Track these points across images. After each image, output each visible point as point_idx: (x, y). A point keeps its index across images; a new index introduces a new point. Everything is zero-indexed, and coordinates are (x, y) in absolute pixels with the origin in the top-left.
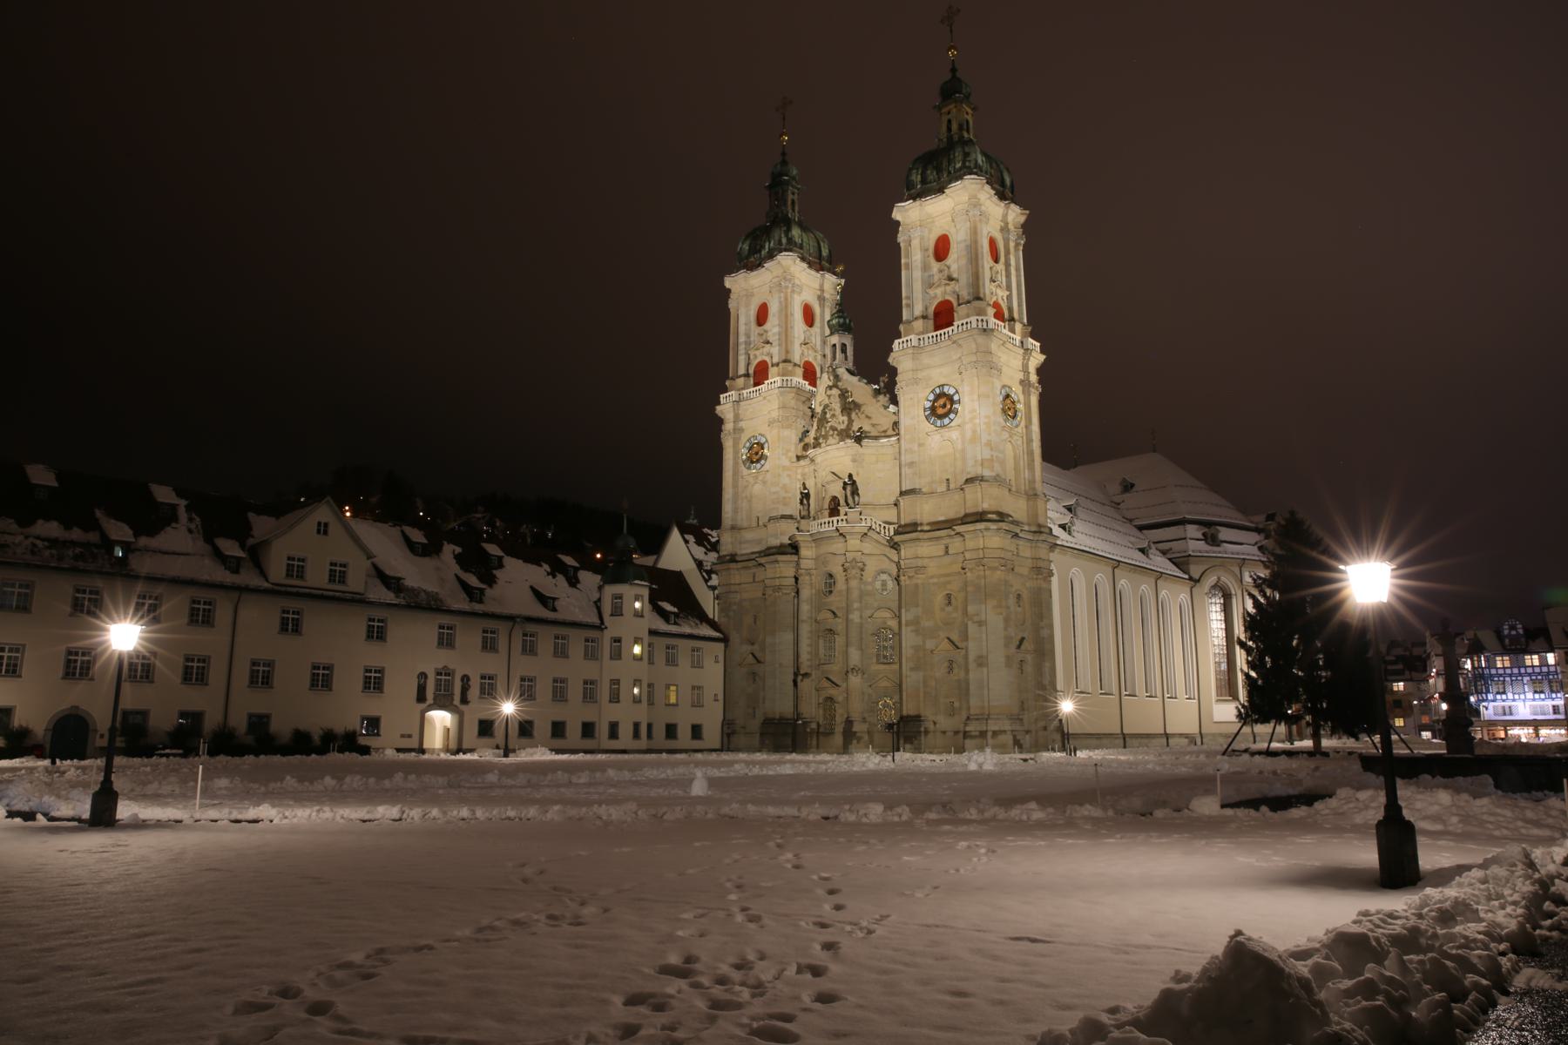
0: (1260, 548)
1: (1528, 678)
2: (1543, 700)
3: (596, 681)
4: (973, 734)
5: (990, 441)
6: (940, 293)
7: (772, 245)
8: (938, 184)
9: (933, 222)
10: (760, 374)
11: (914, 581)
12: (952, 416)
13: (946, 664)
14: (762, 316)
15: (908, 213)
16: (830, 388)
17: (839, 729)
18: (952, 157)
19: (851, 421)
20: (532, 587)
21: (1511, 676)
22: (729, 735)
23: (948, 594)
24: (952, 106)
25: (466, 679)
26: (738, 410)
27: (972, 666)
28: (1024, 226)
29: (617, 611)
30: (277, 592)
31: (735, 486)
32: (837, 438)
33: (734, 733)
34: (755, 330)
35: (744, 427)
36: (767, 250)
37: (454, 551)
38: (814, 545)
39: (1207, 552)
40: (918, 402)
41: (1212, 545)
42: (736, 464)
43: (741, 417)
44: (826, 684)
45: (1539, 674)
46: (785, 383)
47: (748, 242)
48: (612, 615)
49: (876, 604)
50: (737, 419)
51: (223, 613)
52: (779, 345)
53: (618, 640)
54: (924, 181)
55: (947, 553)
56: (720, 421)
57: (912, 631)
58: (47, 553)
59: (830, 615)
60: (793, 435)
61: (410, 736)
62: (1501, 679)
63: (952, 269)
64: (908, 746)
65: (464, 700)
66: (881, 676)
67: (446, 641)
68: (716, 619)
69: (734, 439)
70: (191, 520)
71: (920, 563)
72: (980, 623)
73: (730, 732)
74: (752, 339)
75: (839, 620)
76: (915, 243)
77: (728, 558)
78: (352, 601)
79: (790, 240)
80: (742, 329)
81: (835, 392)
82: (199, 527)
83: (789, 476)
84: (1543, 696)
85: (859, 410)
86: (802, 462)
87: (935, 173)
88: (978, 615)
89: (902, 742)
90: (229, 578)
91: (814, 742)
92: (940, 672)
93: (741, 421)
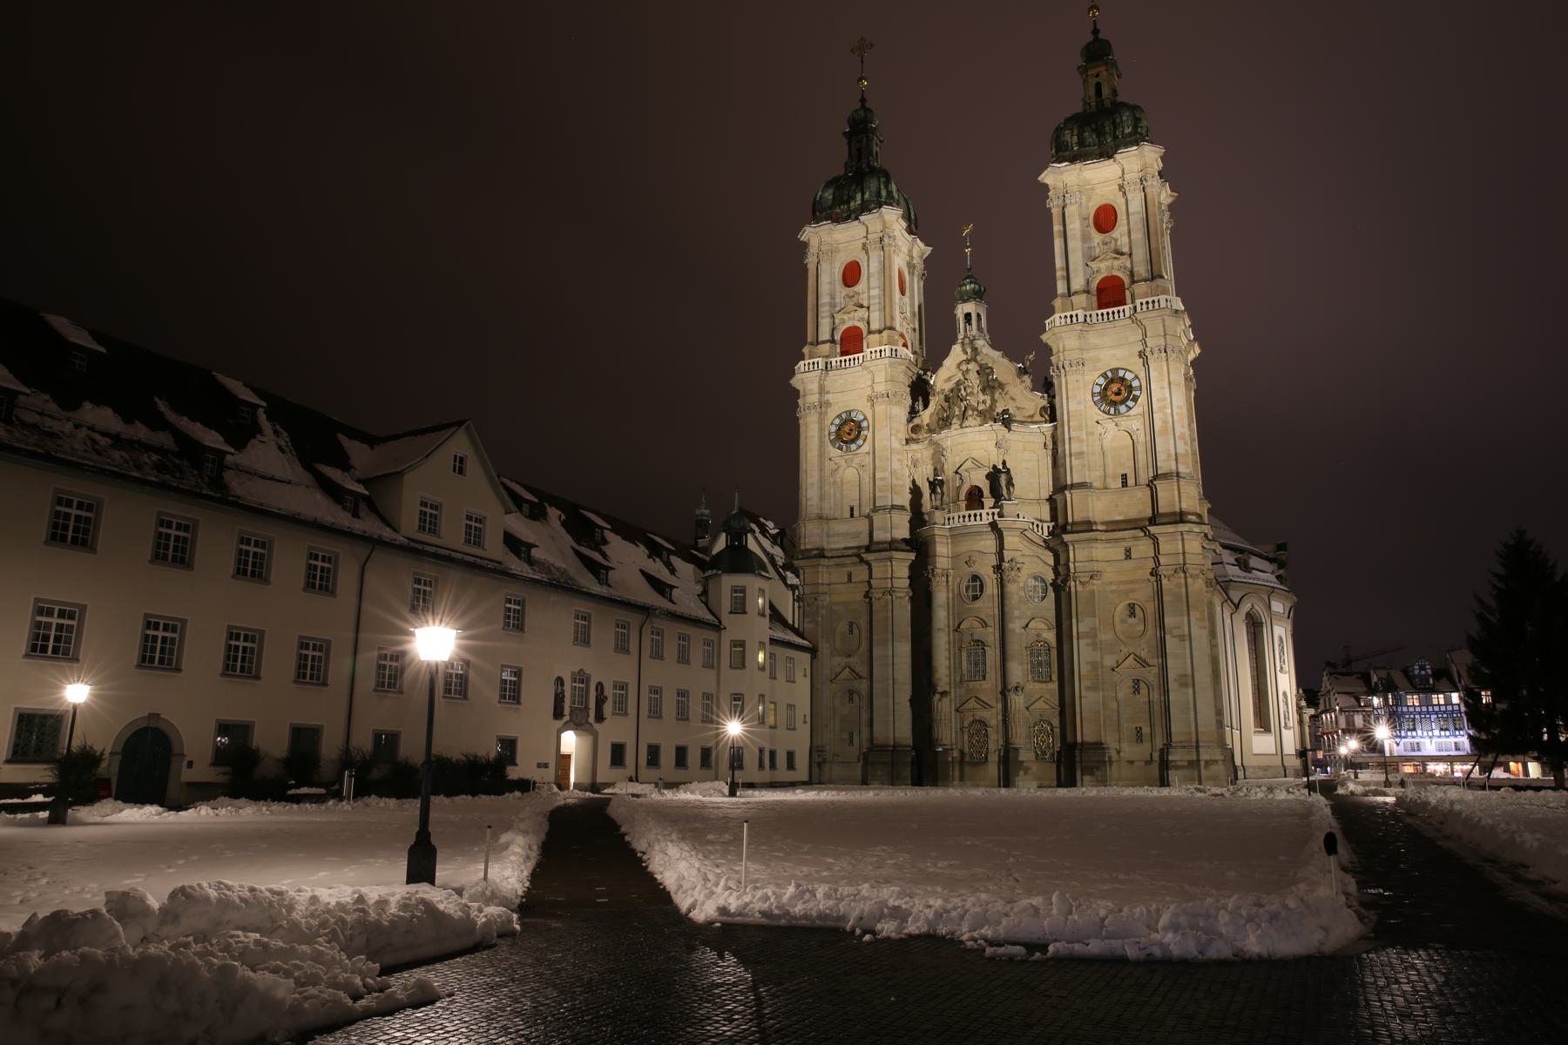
0: (1278, 577)
1: (1435, 716)
2: (1448, 737)
3: (712, 695)
4: (1179, 763)
5: (1183, 434)
6: (1104, 268)
7: (867, 196)
8: (1099, 147)
9: (1093, 189)
10: (851, 342)
11: (1089, 588)
12: (1130, 403)
14: (851, 274)
15: (1061, 177)
16: (968, 361)
17: (993, 758)
18: (1118, 120)
19: (994, 401)
20: (641, 571)
21: (1420, 713)
22: (819, 765)
23: (1129, 605)
24: (1102, 68)
25: (600, 686)
26: (825, 380)
27: (1172, 685)
28: (1170, 206)
29: (740, 607)
30: (413, 550)
31: (821, 470)
32: (978, 419)
33: (824, 761)
34: (842, 291)
35: (831, 401)
36: (859, 202)
37: (560, 516)
38: (949, 541)
39: (1238, 577)
40: (1085, 386)
41: (1245, 571)
42: (821, 442)
43: (827, 389)
44: (972, 704)
45: (1444, 712)
46: (894, 353)
47: (831, 191)
48: (731, 613)
49: (1029, 613)
50: (822, 390)
51: (346, 579)
52: (880, 310)
53: (742, 644)
54: (1081, 143)
55: (1128, 555)
56: (795, 394)
57: (1087, 645)
58: (117, 455)
59: (976, 624)
60: (901, 412)
61: (546, 766)
62: (1412, 716)
63: (1119, 243)
64: (1087, 778)
65: (600, 718)
66: (1037, 696)
67: (583, 638)
68: (796, 625)
69: (821, 413)
70: (276, 432)
71: (1096, 566)
72: (1181, 638)
73: (820, 760)
74: (837, 300)
75: (990, 630)
76: (1071, 210)
77: (815, 552)
78: (494, 571)
79: (890, 193)
80: (825, 288)
81: (973, 366)
82: (290, 444)
83: (899, 460)
84: (1448, 733)
85: (1003, 390)
86: (914, 446)
87: (1094, 137)
88: (1179, 628)
89: (1078, 773)
90: (343, 519)
91: (957, 774)
92: (1124, 691)
93: (828, 393)
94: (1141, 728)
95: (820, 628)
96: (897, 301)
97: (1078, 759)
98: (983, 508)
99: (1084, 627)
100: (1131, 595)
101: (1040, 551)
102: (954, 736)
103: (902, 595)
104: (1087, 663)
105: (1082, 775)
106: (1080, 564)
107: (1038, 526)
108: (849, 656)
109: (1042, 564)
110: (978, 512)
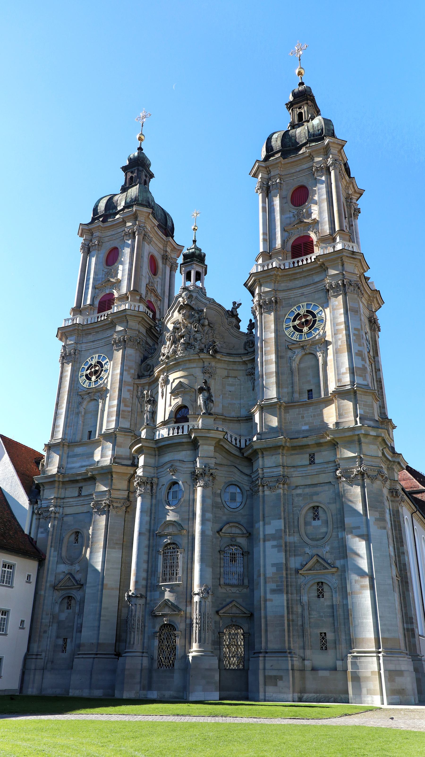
13: (315, 587)
23: (314, 507)
49: (225, 518)
55: (312, 462)
57: (273, 547)
66: (228, 600)
68: (32, 536)
94: (325, 633)
95: (50, 538)
97: (261, 666)
99: (270, 530)
100: (315, 498)
102: (146, 640)
103: (119, 505)
104: (273, 565)
105: (265, 685)
106: (268, 470)
107: (236, 440)
108: (72, 564)
109: (238, 473)
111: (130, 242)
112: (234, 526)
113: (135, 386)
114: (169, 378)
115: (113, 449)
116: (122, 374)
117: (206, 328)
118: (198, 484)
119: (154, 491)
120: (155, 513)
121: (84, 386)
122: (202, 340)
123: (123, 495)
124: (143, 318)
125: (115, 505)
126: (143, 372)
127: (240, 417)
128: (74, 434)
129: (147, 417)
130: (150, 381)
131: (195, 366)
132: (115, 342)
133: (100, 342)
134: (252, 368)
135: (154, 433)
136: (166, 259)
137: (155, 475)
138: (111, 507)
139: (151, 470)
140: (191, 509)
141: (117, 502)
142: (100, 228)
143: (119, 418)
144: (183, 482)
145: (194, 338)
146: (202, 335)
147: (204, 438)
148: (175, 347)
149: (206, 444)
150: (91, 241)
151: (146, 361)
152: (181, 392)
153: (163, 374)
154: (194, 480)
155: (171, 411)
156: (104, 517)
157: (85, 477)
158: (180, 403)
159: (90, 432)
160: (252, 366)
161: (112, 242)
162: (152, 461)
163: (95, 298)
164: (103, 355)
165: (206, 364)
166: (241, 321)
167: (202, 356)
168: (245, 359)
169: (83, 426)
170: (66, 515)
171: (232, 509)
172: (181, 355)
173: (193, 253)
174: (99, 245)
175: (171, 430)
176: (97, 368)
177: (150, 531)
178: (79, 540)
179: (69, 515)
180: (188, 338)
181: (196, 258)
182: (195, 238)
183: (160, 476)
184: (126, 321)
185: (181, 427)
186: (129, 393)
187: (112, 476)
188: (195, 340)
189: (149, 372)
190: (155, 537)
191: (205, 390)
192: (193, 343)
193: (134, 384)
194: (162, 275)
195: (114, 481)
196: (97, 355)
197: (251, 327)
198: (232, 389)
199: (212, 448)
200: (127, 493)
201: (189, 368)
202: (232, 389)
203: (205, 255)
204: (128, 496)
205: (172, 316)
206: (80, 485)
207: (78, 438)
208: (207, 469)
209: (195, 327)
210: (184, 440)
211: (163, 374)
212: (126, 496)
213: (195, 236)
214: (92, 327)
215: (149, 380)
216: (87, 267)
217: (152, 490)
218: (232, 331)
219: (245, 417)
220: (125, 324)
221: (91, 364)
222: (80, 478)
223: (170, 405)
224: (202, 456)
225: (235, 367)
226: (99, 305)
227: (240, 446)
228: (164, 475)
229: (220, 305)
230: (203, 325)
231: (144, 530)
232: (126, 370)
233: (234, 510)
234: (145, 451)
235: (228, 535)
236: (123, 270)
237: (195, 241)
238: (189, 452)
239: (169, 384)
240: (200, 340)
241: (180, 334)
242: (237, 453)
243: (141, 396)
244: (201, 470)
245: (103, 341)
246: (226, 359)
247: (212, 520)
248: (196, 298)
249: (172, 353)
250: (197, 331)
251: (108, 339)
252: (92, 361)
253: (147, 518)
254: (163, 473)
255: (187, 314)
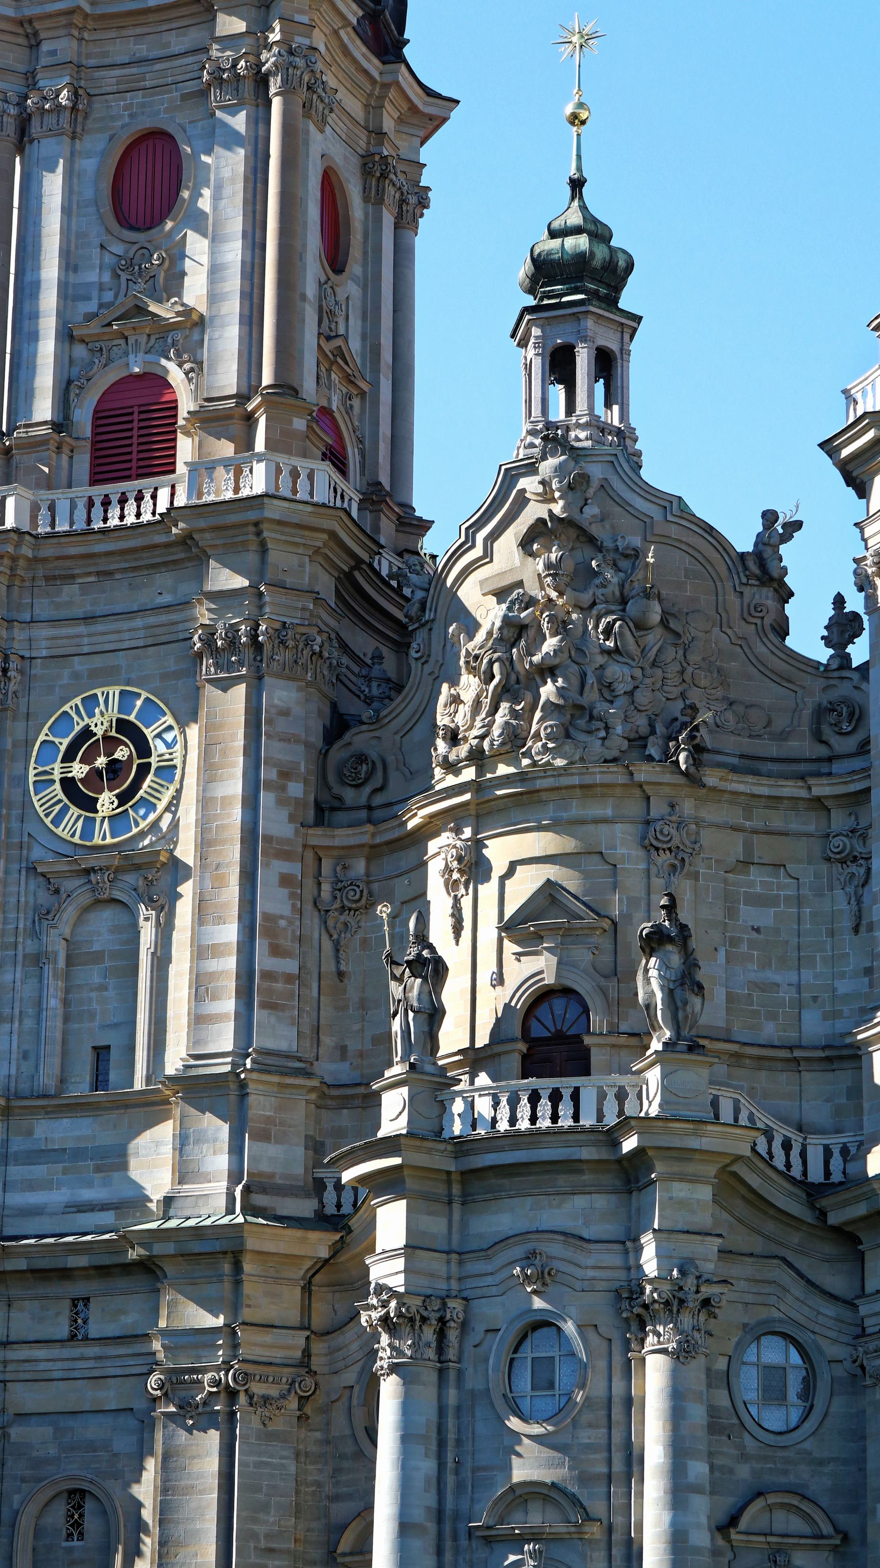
49: (743, 1471)
96: (311, 290)
98: (586, 1072)
101: (795, 1238)
103: (273, 1391)
107: (787, 1146)
109: (797, 1289)
110: (566, 1084)
111: (239, 122)
112: (783, 1506)
113: (309, 855)
114: (484, 851)
115: (236, 1149)
116: (250, 802)
117: (654, 638)
118: (651, 1339)
119: (452, 1353)
120: (459, 1442)
121: (59, 831)
122: (638, 694)
123: (289, 1347)
124: (333, 535)
125: (258, 1389)
126: (337, 789)
127: (800, 1047)
128: (25, 1056)
129: (406, 1032)
130: (378, 840)
131: (609, 812)
132: (209, 641)
133: (125, 625)
134: (853, 831)
135: (443, 1107)
136: (384, 176)
137: (454, 1285)
138: (242, 1399)
139: (435, 1263)
140: (617, 1437)
141: (264, 1379)
142: (77, 19)
143: (249, 1006)
144: (580, 1327)
145: (600, 680)
146: (638, 673)
147: (674, 1154)
148: (514, 713)
149: (682, 1178)
150: (30, 79)
151: (347, 737)
152: (554, 929)
153: (458, 831)
154: (627, 1320)
155: (507, 1006)
156: (213, 1438)
157: (107, 1260)
158: (549, 979)
159: (101, 1053)
160: (851, 822)
161: (138, 98)
162: (436, 1225)
163: (74, 391)
164: (145, 694)
165: (658, 808)
166: (792, 594)
167: (644, 772)
168: (822, 788)
169: (66, 1019)
170: (22, 1416)
171: (771, 1436)
172: (546, 758)
173: (581, 260)
174: (74, 109)
175: (524, 1101)
176: (121, 754)
177: (439, 1515)
178: (92, 1523)
179: (34, 1419)
180: (576, 681)
181: (593, 280)
182: (579, 169)
183: (479, 1293)
184: (254, 547)
185: (567, 1094)
186: (285, 891)
187: (237, 1267)
188: (607, 688)
189: (367, 790)
190: (464, 1542)
191: (670, 940)
192: (601, 707)
193: (305, 846)
194: (365, 265)
195: (248, 1288)
196: (115, 691)
197: (843, 632)
198: (765, 917)
199: (705, 1193)
200: (302, 1342)
201: (582, 822)
202: (765, 917)
203: (630, 267)
204: (307, 1353)
205: (488, 555)
206: (79, 1288)
207: (47, 1078)
208: (690, 1283)
209: (608, 632)
210: (587, 1153)
211: (458, 831)
212: (298, 1354)
213: (579, 157)
214: (81, 550)
215: (373, 835)
216: (15, 212)
217: (441, 1349)
218: (761, 649)
219: (824, 1048)
220: (251, 558)
221: (87, 733)
222: (82, 1261)
223: (499, 979)
224: (668, 1225)
225: (776, 820)
226: (95, 426)
227: (805, 1173)
228: (494, 1291)
229: (710, 530)
230: (640, 626)
231: (418, 1515)
232: (268, 785)
233: (782, 1440)
234: (409, 1183)
235: (762, 1539)
236: (215, 271)
237: (577, 185)
238: (601, 1202)
239: (487, 878)
240: (630, 694)
241: (536, 659)
242: (795, 1207)
243: (337, 905)
244: (666, 1287)
245: (138, 622)
246: (741, 788)
247: (708, 1488)
248: (604, 486)
249: (503, 744)
250: (617, 650)
251: (163, 618)
252: (91, 715)
253: (427, 1466)
254: (489, 1280)
255: (569, 566)
